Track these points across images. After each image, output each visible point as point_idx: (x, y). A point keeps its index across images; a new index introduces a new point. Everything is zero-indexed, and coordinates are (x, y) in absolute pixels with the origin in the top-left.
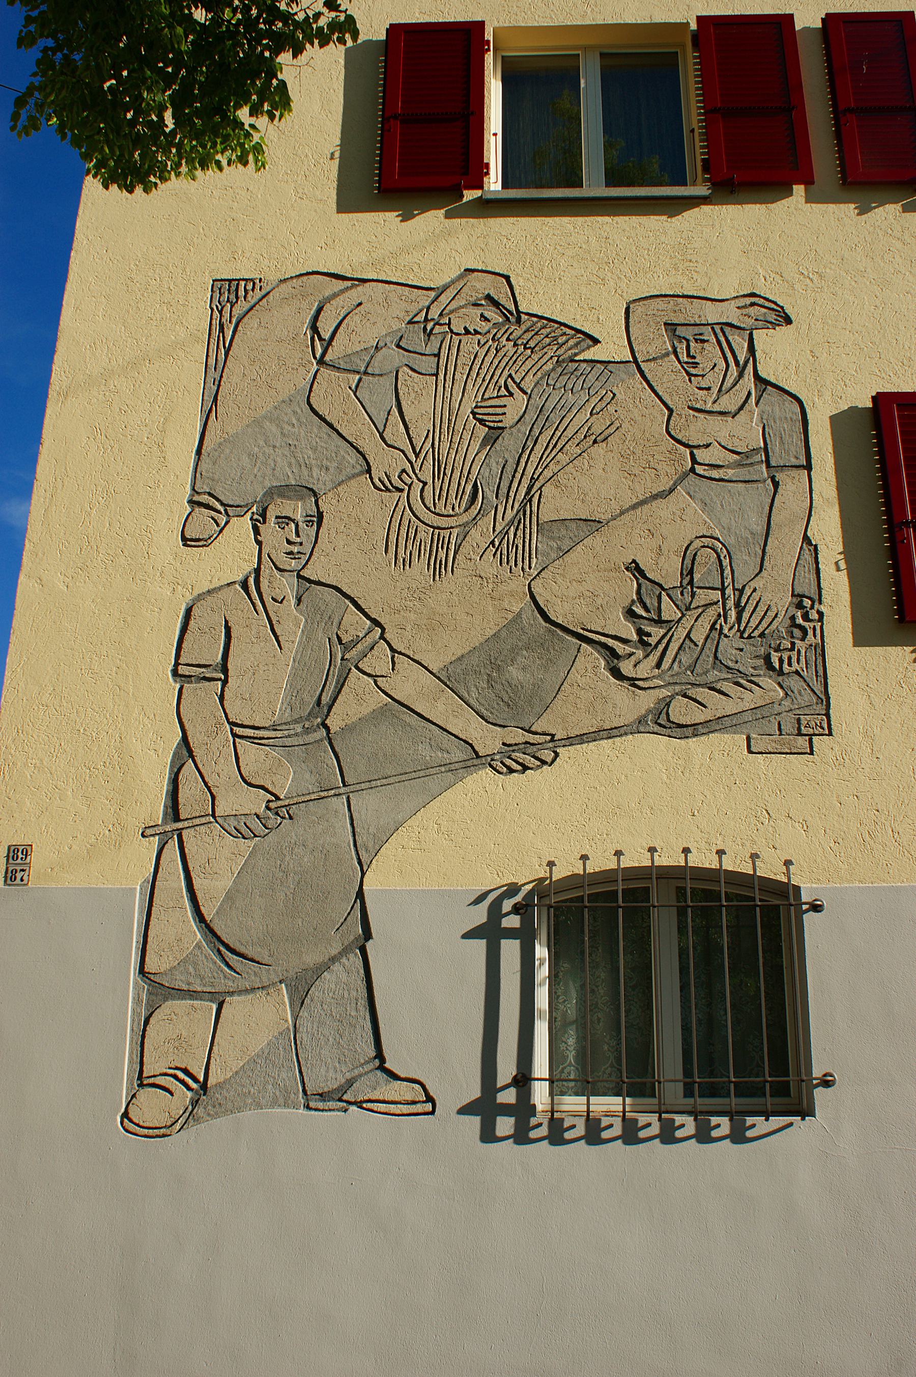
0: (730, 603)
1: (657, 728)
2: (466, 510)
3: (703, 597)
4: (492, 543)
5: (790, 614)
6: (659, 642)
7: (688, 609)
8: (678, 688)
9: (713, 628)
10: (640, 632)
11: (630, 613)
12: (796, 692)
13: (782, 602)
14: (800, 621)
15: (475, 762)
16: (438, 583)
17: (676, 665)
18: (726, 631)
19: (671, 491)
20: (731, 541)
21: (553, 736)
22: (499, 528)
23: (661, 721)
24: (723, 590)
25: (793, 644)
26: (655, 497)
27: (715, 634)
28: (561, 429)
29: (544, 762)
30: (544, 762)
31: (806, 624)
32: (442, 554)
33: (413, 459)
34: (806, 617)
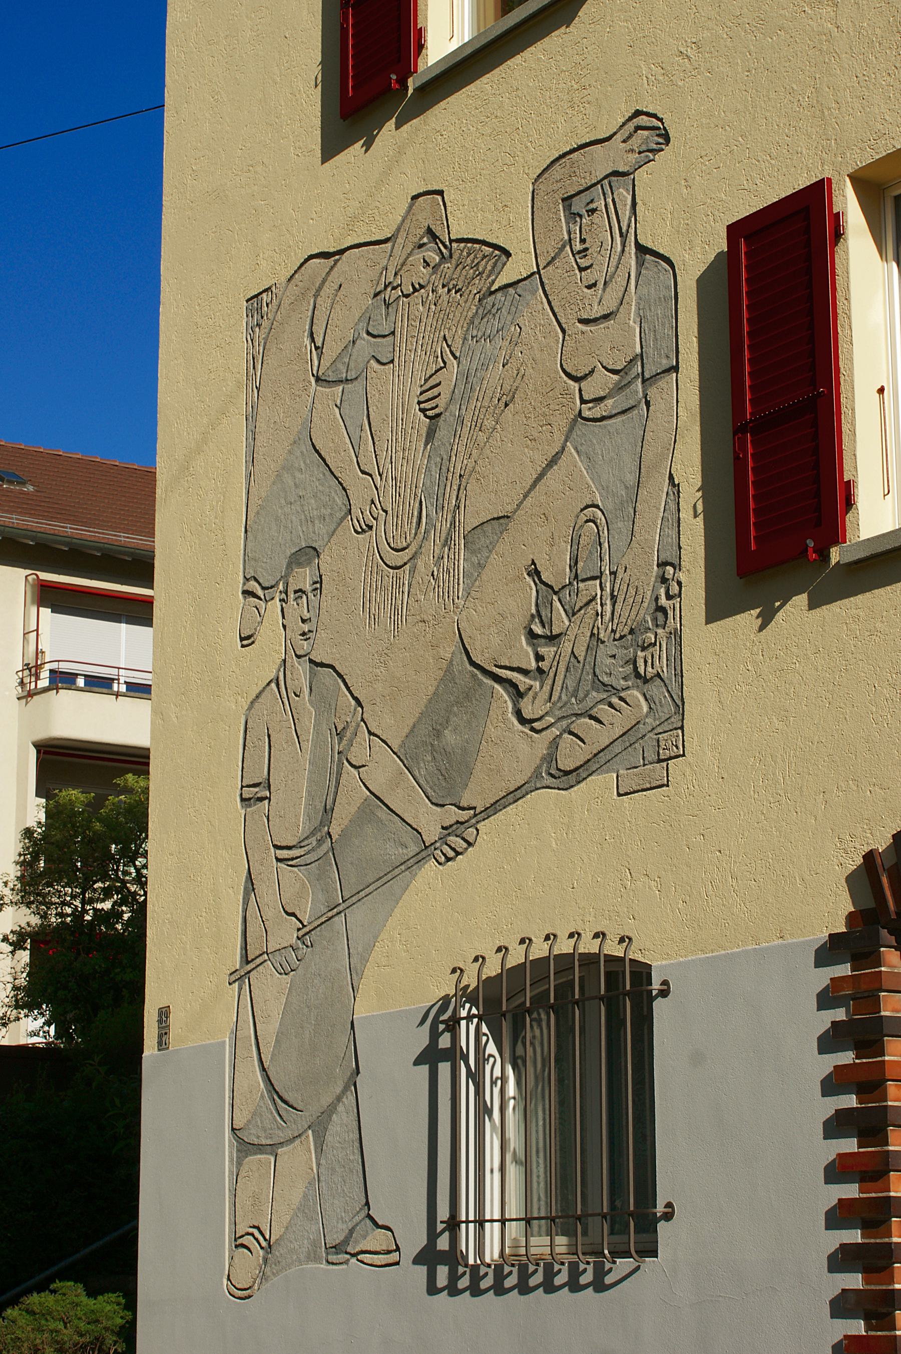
1: (549, 781)
12: (657, 702)
14: (663, 601)
21: (475, 808)
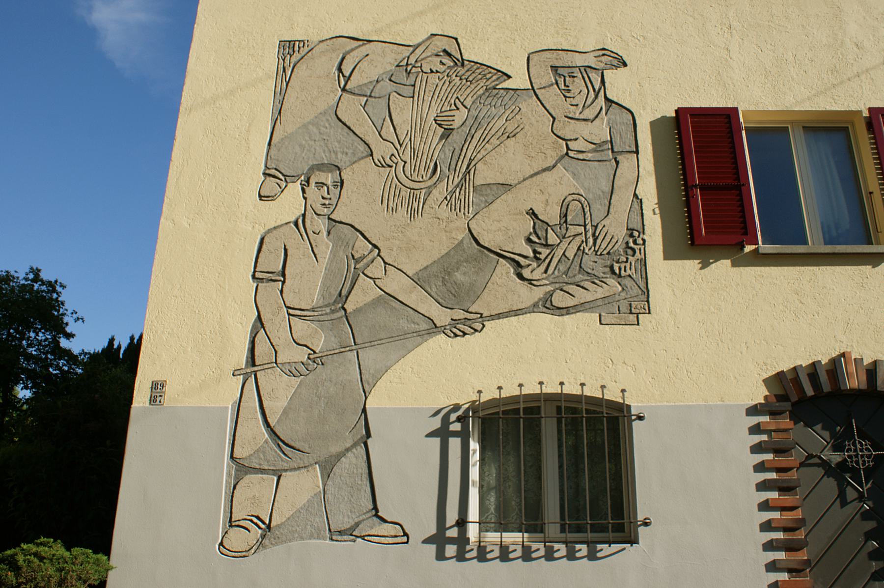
0: (590, 234)
1: (545, 310)
2: (430, 178)
3: (573, 230)
4: (446, 198)
5: (625, 241)
6: (546, 258)
7: (564, 237)
8: (557, 286)
9: (579, 249)
10: (535, 252)
11: (529, 240)
13: (621, 234)
14: (631, 245)
15: (435, 330)
16: (413, 222)
17: (556, 272)
18: (587, 251)
19: (554, 166)
20: (590, 196)
21: (482, 314)
22: (449, 190)
23: (547, 305)
24: (585, 226)
25: (627, 259)
26: (544, 170)
27: (580, 253)
28: (488, 129)
29: (476, 330)
30: (476, 330)
31: (635, 247)
32: (415, 205)
33: (398, 147)
34: (635, 242)
